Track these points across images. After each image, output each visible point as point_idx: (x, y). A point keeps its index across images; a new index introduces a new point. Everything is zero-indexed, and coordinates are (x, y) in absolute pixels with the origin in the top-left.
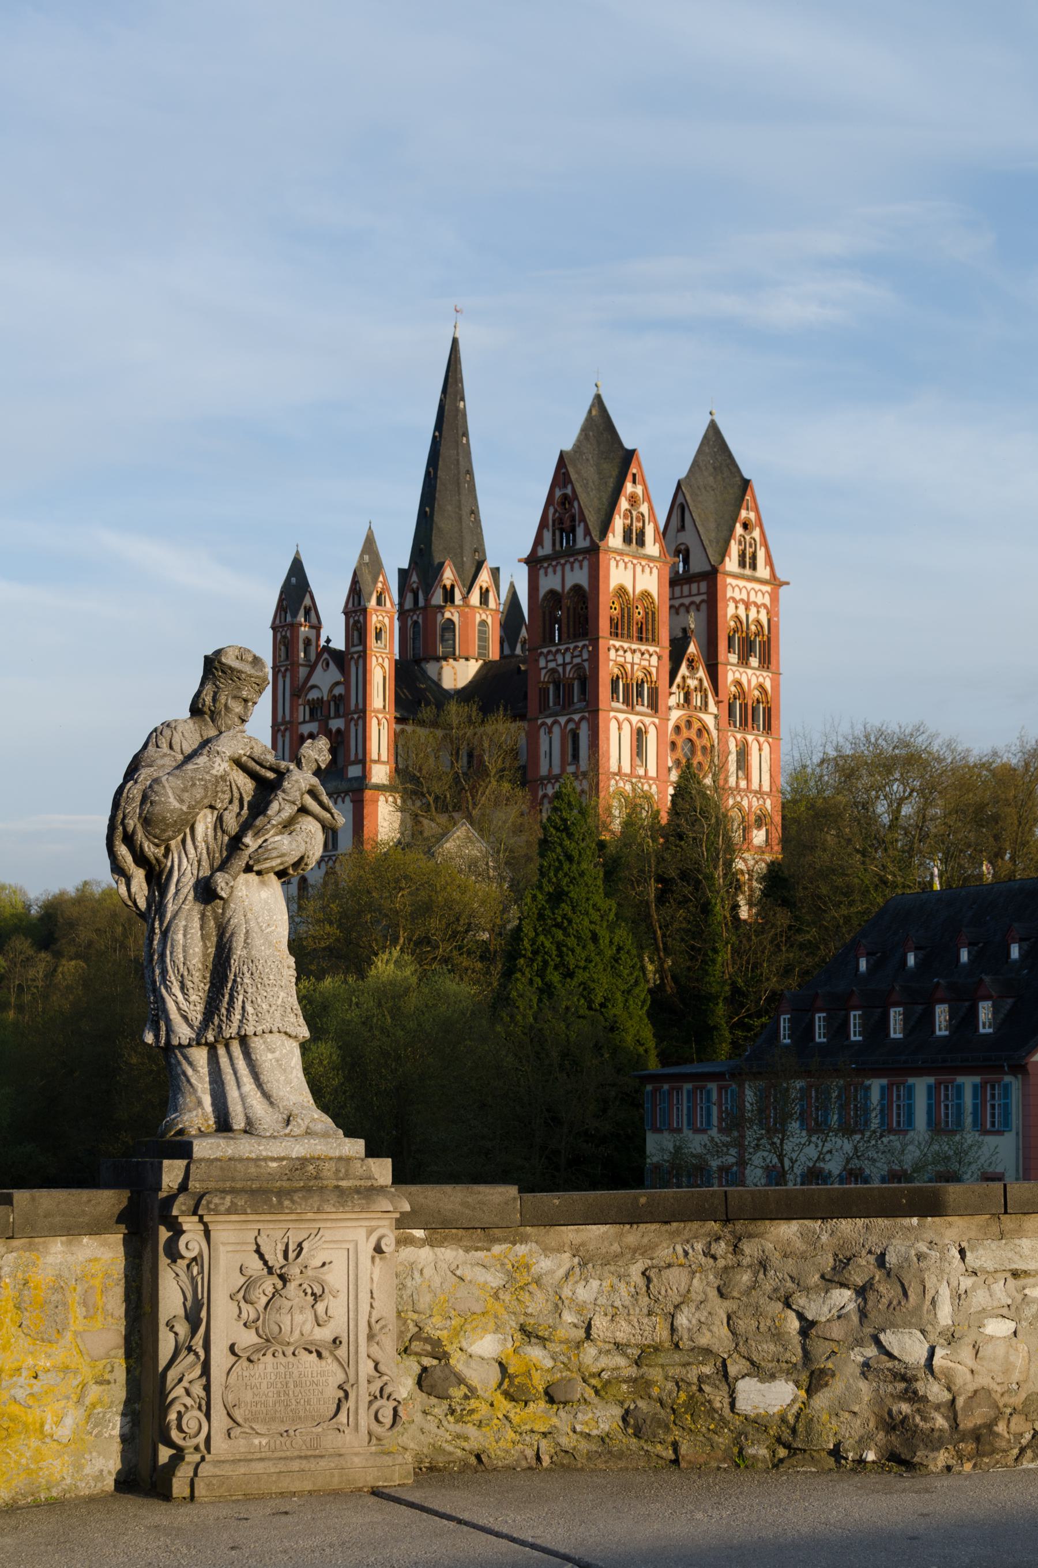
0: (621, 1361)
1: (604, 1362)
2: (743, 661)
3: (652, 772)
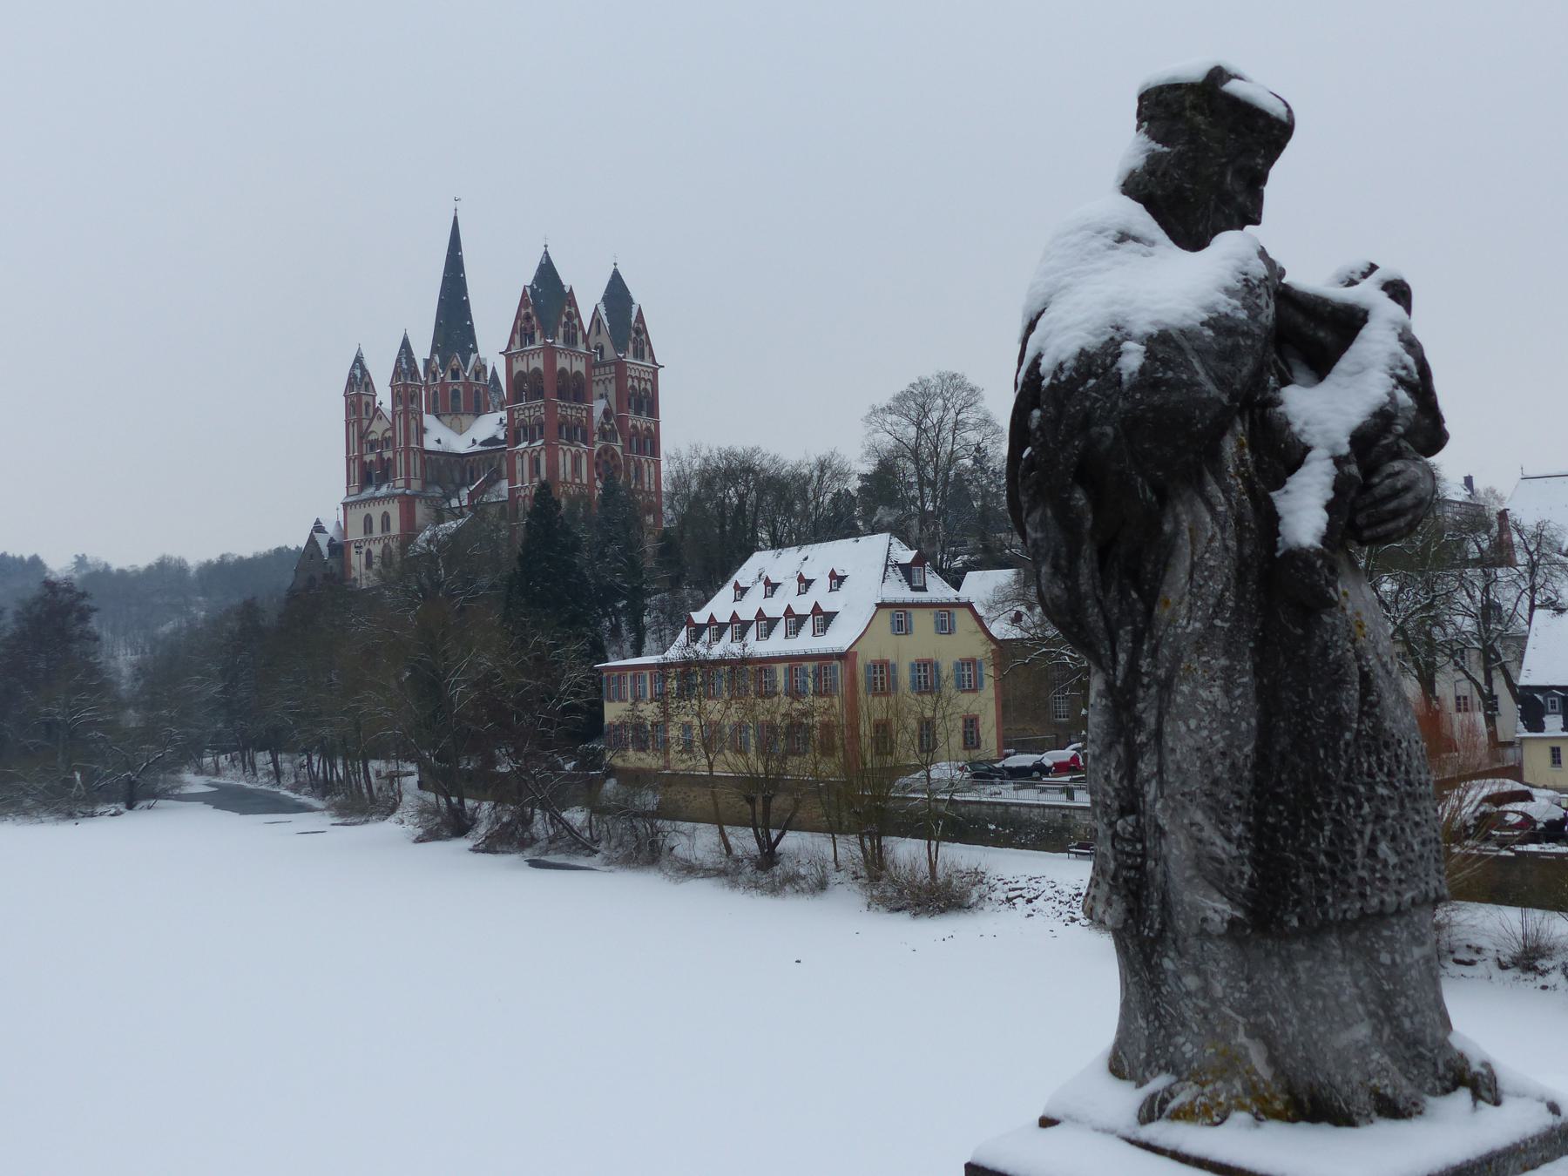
2: (638, 412)
3: (585, 481)
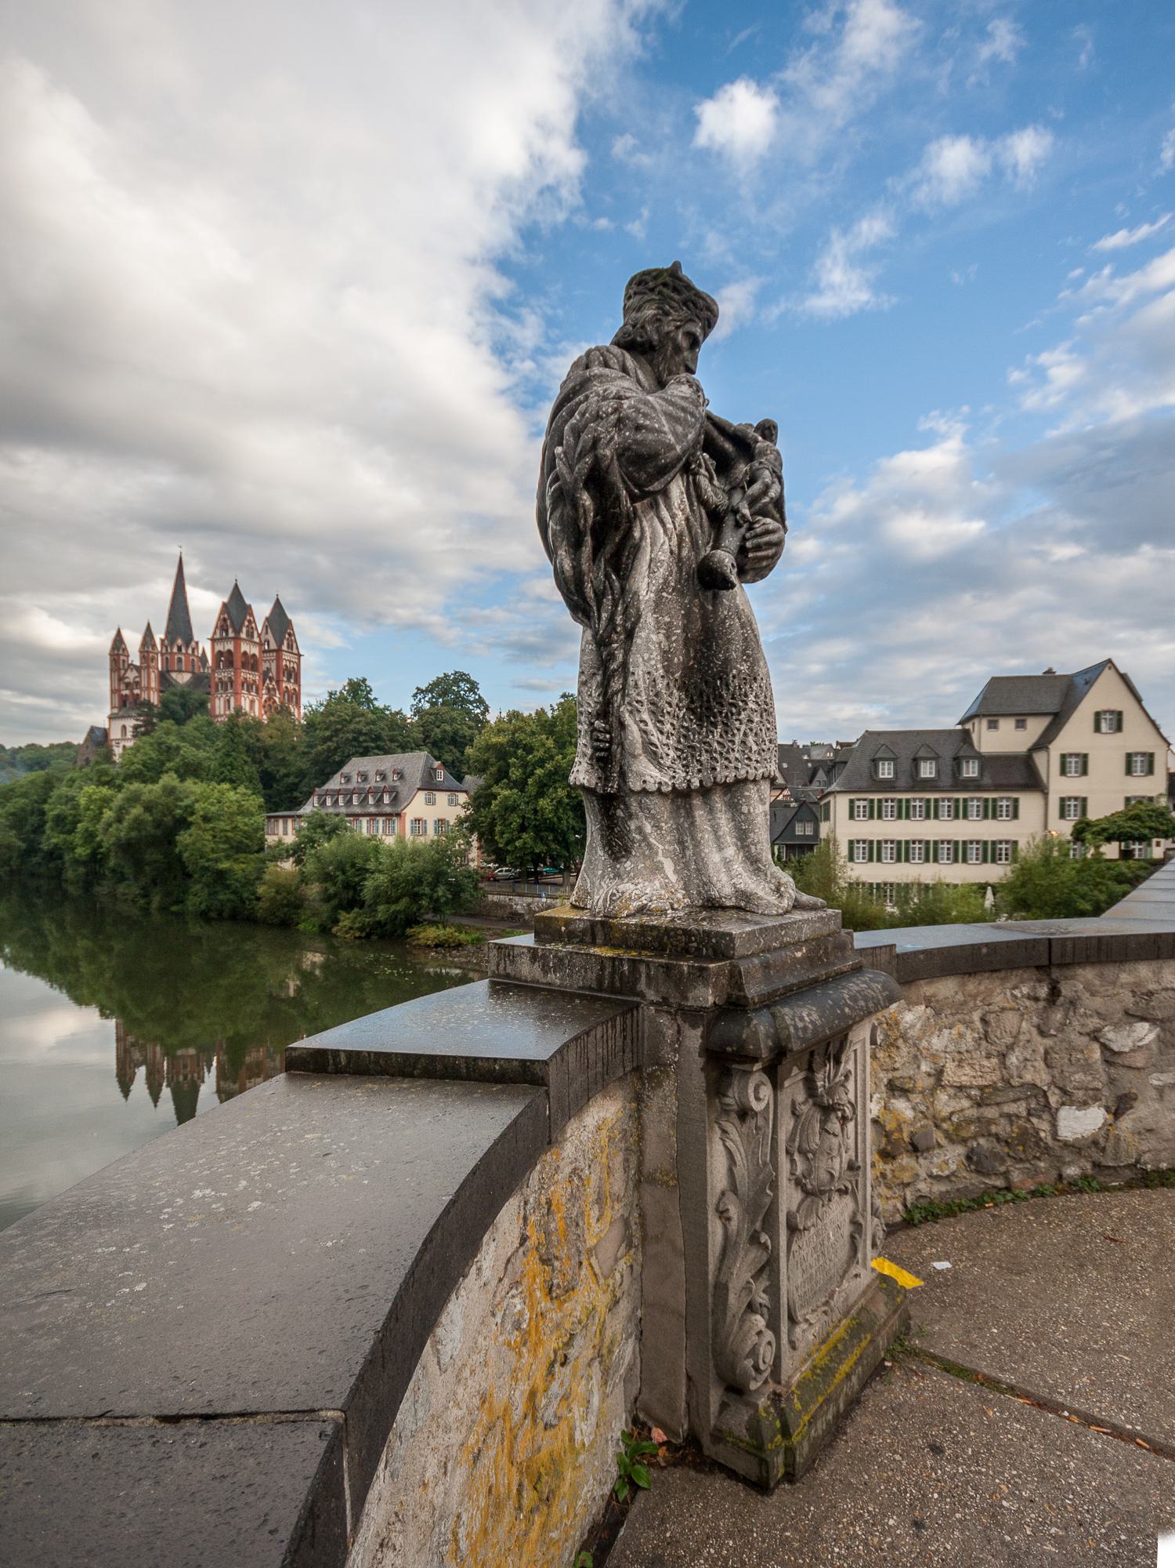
0: (966, 1103)
1: (955, 1105)
